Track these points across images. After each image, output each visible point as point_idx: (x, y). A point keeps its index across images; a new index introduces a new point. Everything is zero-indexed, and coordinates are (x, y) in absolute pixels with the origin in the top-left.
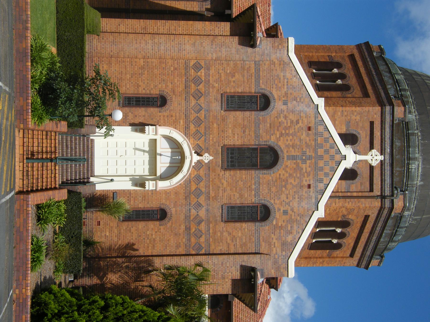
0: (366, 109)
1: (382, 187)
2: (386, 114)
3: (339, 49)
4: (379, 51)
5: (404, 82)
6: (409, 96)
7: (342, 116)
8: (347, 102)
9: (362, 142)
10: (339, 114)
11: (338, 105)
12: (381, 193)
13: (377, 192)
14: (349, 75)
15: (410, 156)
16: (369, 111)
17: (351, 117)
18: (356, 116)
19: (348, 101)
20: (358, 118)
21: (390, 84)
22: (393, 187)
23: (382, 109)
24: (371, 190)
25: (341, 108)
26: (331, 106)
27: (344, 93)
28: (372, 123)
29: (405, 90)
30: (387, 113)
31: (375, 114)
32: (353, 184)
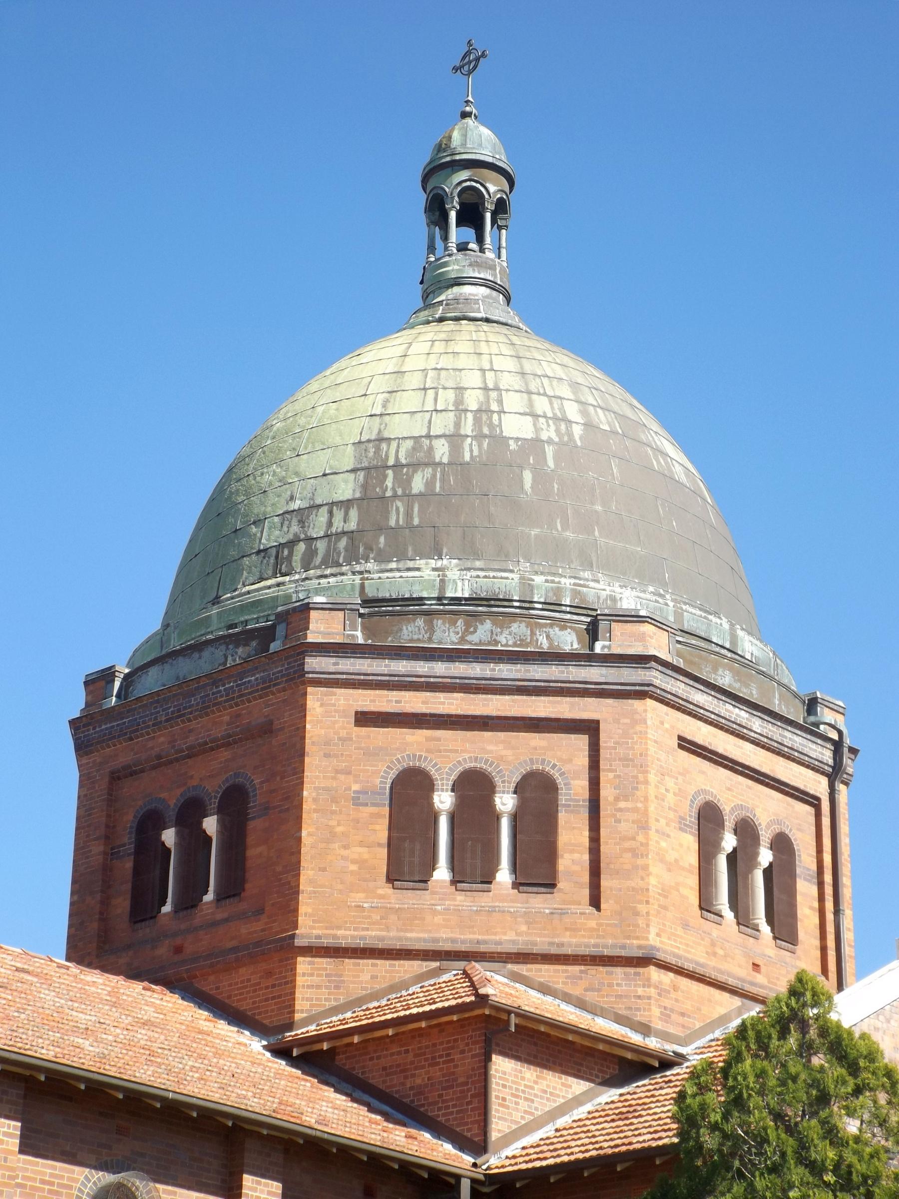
0: (652, 749)
1: (814, 769)
2: (668, 688)
3: (327, 755)
4: (340, 614)
5: (485, 577)
6: (553, 582)
7: (668, 836)
8: (622, 805)
9: (715, 792)
10: (663, 844)
11: (641, 838)
12: (823, 773)
13: (818, 785)
14: (467, 756)
15: (727, 645)
16: (656, 742)
17: (670, 808)
18: (667, 790)
19: (617, 799)
20: (670, 783)
21: (533, 634)
22: (812, 731)
23: (651, 697)
24: (813, 801)
25: (652, 833)
26: (645, 868)
27: (562, 799)
28: (687, 745)
29: (526, 584)
30: (664, 686)
31: (662, 723)
32: (800, 856)
